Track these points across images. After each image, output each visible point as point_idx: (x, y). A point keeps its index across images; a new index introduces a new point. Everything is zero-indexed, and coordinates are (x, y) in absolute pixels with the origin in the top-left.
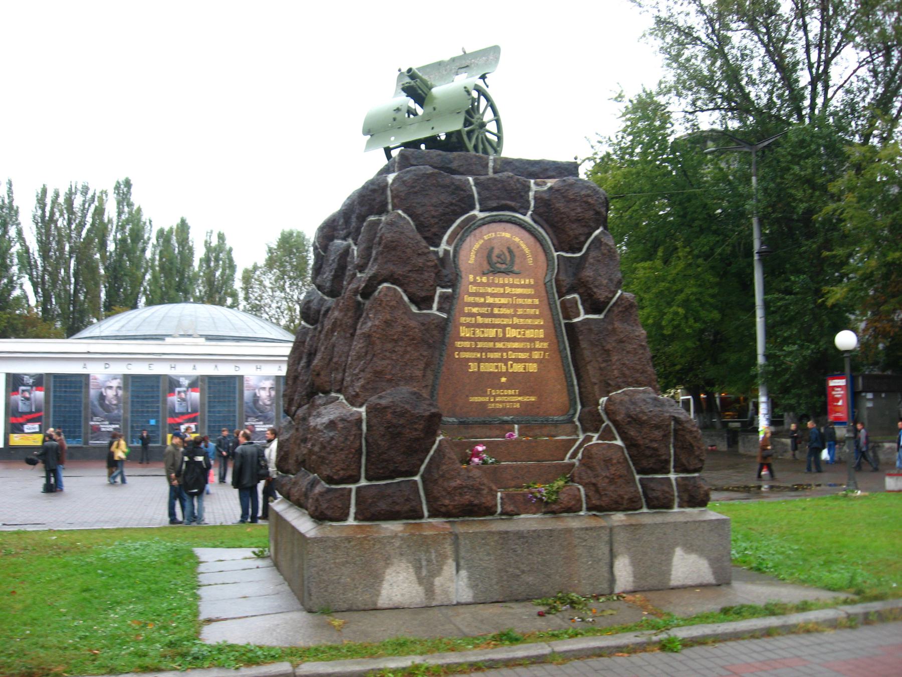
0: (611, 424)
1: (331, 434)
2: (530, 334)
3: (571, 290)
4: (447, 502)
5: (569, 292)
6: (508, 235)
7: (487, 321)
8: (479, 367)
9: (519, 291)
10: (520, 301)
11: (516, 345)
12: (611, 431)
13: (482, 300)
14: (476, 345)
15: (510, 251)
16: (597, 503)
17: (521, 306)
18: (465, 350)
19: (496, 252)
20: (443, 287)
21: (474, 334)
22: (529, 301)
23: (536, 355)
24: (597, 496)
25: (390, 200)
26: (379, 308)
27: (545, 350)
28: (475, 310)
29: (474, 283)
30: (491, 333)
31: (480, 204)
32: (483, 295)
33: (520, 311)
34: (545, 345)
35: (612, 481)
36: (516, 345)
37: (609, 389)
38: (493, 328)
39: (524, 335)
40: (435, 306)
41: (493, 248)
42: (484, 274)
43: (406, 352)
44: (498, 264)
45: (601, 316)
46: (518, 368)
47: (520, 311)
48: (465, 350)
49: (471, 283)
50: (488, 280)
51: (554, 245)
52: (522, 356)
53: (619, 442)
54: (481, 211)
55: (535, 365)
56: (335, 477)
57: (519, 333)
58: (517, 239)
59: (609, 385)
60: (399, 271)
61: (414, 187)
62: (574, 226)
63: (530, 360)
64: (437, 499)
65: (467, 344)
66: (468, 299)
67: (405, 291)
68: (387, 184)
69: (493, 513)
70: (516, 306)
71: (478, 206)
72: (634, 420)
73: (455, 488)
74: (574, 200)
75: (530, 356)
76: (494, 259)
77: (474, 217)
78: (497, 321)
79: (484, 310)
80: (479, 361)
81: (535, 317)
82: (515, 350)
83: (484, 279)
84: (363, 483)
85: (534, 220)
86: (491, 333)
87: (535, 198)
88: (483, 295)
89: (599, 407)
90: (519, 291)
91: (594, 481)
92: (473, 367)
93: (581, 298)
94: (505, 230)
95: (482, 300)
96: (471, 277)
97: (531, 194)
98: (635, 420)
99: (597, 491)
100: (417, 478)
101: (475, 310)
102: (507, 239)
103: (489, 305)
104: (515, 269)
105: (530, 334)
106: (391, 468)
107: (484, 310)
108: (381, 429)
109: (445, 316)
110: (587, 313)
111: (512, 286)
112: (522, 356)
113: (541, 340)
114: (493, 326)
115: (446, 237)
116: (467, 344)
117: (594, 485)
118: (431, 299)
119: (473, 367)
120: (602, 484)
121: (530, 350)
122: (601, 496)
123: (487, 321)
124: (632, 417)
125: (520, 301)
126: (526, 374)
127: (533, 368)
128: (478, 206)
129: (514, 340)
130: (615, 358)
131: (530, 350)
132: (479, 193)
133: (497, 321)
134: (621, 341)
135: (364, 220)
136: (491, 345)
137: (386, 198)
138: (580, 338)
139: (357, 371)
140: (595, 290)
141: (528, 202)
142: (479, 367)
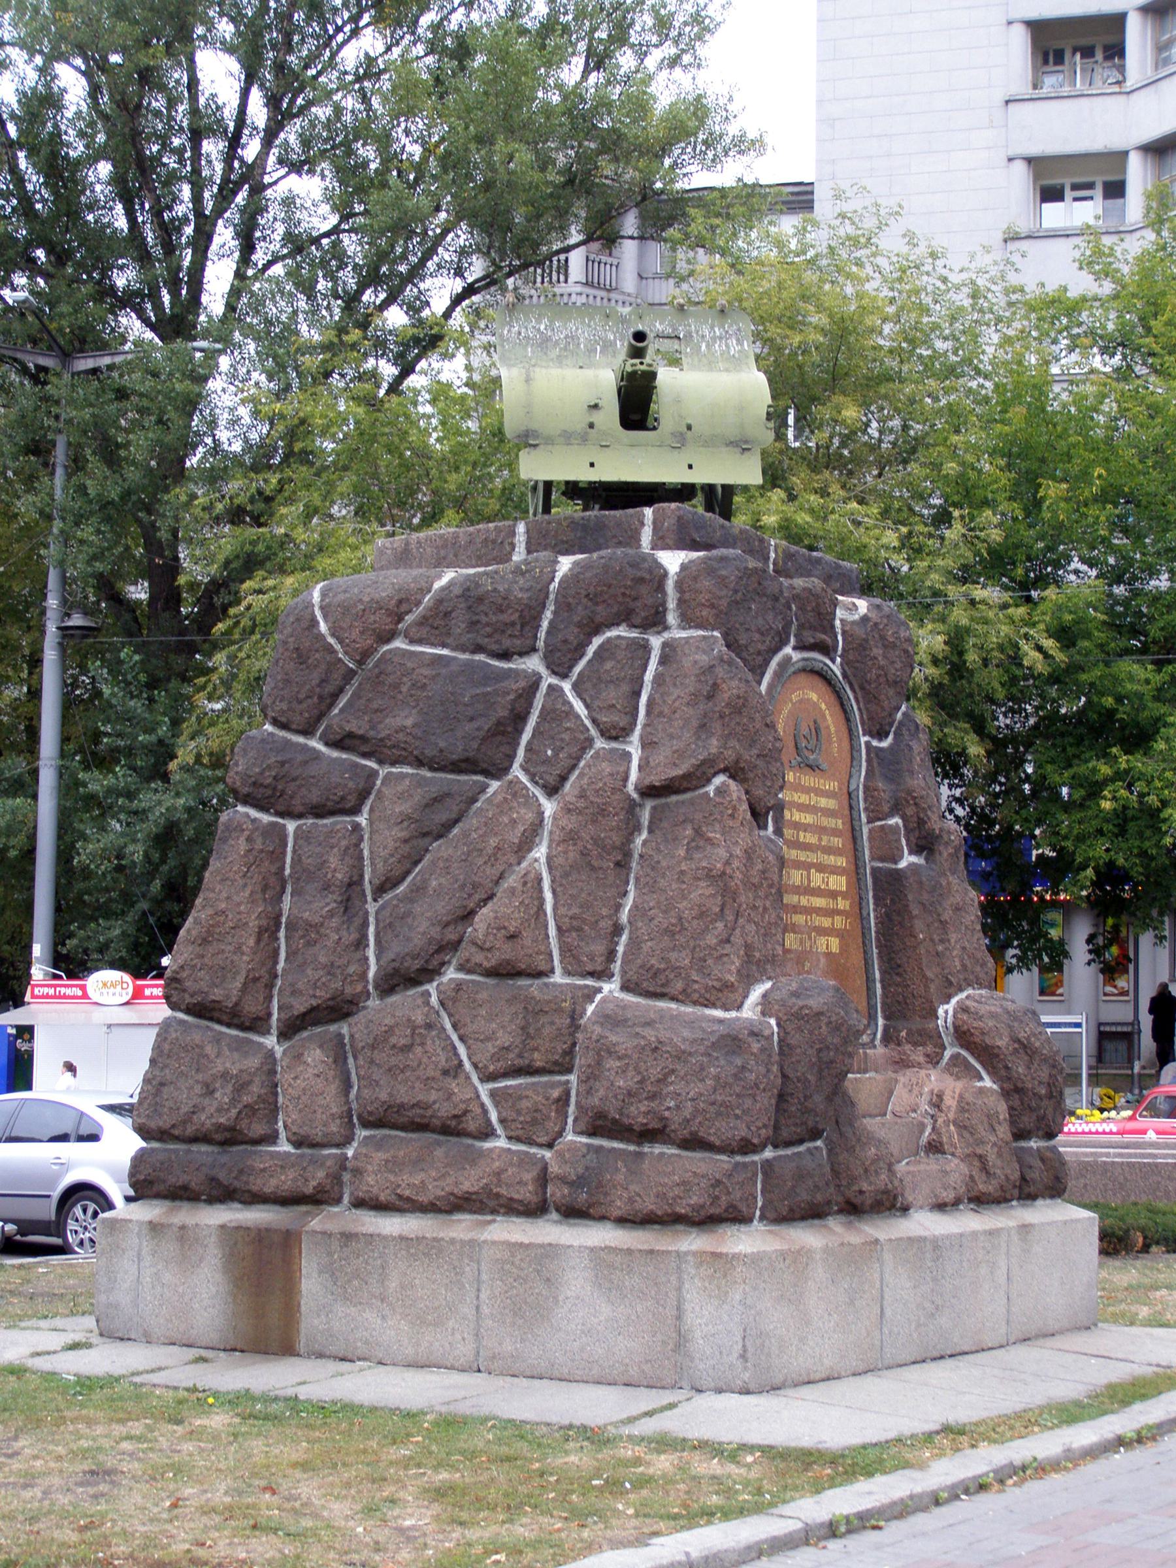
0: (964, 1053)
1: (739, 1062)
3: (896, 809)
4: (865, 1186)
5: (890, 815)
6: (814, 697)
12: (968, 1066)
16: (982, 1187)
24: (984, 1177)
25: (671, 604)
26: (731, 823)
35: (1000, 1155)
37: (951, 990)
43: (765, 909)
51: (863, 724)
53: (988, 1083)
54: (794, 648)
56: (755, 1141)
58: (823, 706)
59: (951, 983)
60: (750, 755)
61: (736, 591)
62: (891, 692)
64: (853, 1179)
68: (666, 574)
69: (892, 1207)
72: (1024, 1048)
73: (874, 1162)
74: (894, 646)
78: (803, 856)
82: (819, 911)
84: (769, 1153)
87: (844, 633)
91: (979, 1151)
94: (812, 689)
97: (838, 623)
98: (1025, 1047)
99: (984, 1169)
100: (819, 1143)
106: (810, 1124)
108: (810, 1052)
110: (911, 853)
117: (980, 1156)
120: (992, 1158)
122: (988, 1173)
124: (1019, 1041)
126: (828, 955)
128: (792, 639)
130: (953, 937)
134: (957, 909)
135: (597, 631)
137: (664, 604)
138: (910, 897)
139: (711, 940)
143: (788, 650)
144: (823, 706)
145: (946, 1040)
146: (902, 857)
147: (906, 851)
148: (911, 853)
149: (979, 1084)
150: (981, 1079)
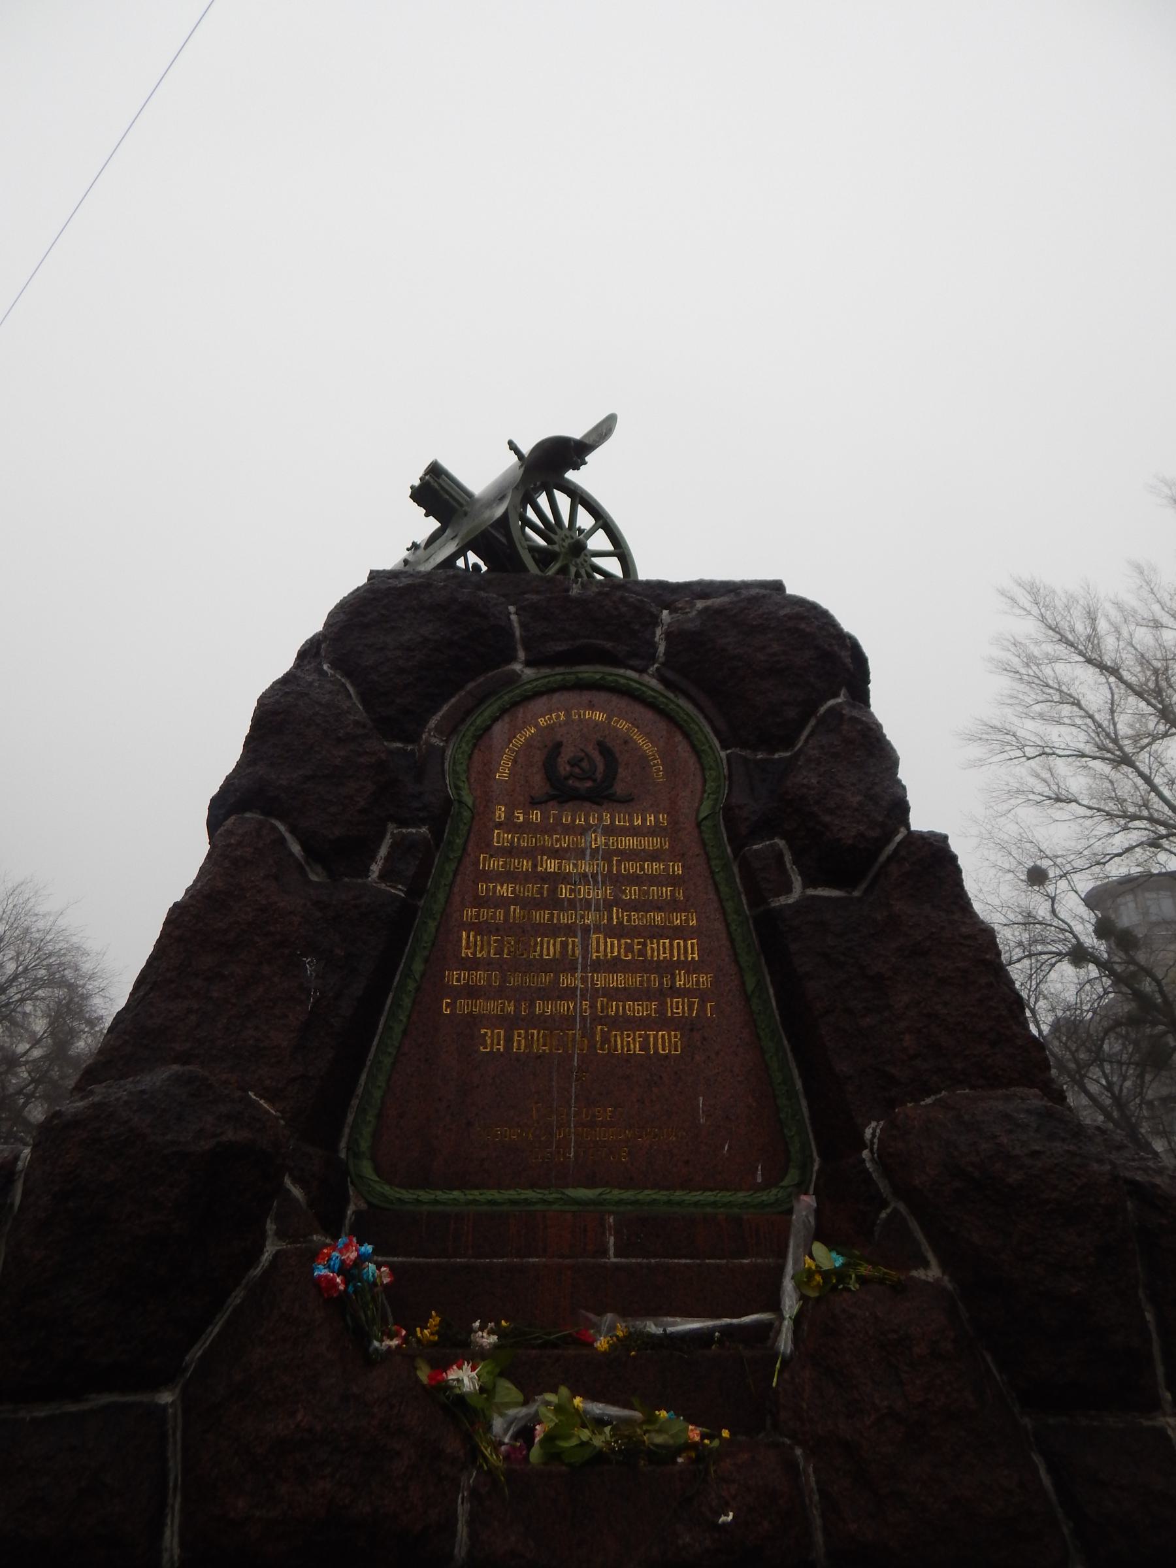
0: (902, 1207)
2: (659, 950)
3: (766, 826)
6: (599, 716)
7: (542, 916)
8: (509, 1040)
9: (630, 842)
10: (631, 867)
11: (617, 980)
13: (526, 865)
14: (504, 980)
15: (604, 750)
17: (635, 880)
18: (472, 992)
19: (567, 753)
20: (403, 823)
21: (499, 952)
22: (656, 868)
23: (677, 1008)
27: (704, 996)
28: (505, 890)
29: (509, 825)
30: (550, 949)
31: (527, 649)
32: (530, 854)
33: (631, 893)
34: (705, 980)
36: (617, 980)
38: (555, 936)
39: (642, 953)
40: (375, 868)
41: (559, 745)
42: (534, 803)
44: (580, 781)
45: (856, 894)
46: (628, 1043)
47: (631, 893)
48: (472, 992)
49: (499, 825)
50: (545, 817)
52: (638, 1010)
53: (933, 1273)
54: (528, 663)
55: (675, 1037)
57: (629, 949)
58: (623, 725)
63: (663, 1022)
65: (480, 977)
66: (495, 864)
67: (293, 830)
70: (617, 881)
71: (521, 655)
75: (661, 1010)
76: (564, 768)
77: (514, 678)
79: (531, 890)
80: (510, 1023)
81: (673, 906)
82: (612, 994)
83: (536, 816)
85: (663, 680)
86: (550, 949)
87: (668, 636)
88: (530, 854)
89: (865, 1154)
90: (630, 842)
92: (492, 1041)
93: (791, 847)
94: (591, 706)
95: (526, 865)
96: (500, 813)
100: (166, 1398)
101: (505, 890)
102: (597, 724)
103: (545, 877)
104: (619, 789)
105: (659, 950)
107: (531, 890)
109: (400, 891)
111: (610, 831)
112: (638, 1010)
113: (690, 967)
114: (554, 930)
115: (432, 723)
116: (480, 977)
118: (362, 850)
119: (492, 1041)
121: (661, 995)
123: (542, 916)
125: (631, 867)
127: (665, 1042)
128: (521, 655)
129: (614, 965)
131: (661, 995)
132: (523, 625)
133: (565, 919)
136: (545, 979)
140: (827, 819)
141: (654, 646)
142: (509, 1040)
143: (517, 667)
144: (623, 725)
145: (883, 1186)
146: (789, 890)
147: (797, 882)
148: (809, 882)
149: (919, 1274)
150: (926, 1265)
